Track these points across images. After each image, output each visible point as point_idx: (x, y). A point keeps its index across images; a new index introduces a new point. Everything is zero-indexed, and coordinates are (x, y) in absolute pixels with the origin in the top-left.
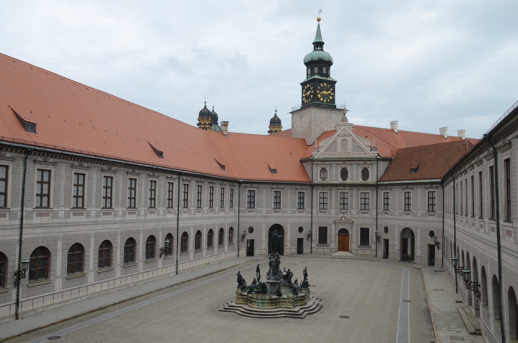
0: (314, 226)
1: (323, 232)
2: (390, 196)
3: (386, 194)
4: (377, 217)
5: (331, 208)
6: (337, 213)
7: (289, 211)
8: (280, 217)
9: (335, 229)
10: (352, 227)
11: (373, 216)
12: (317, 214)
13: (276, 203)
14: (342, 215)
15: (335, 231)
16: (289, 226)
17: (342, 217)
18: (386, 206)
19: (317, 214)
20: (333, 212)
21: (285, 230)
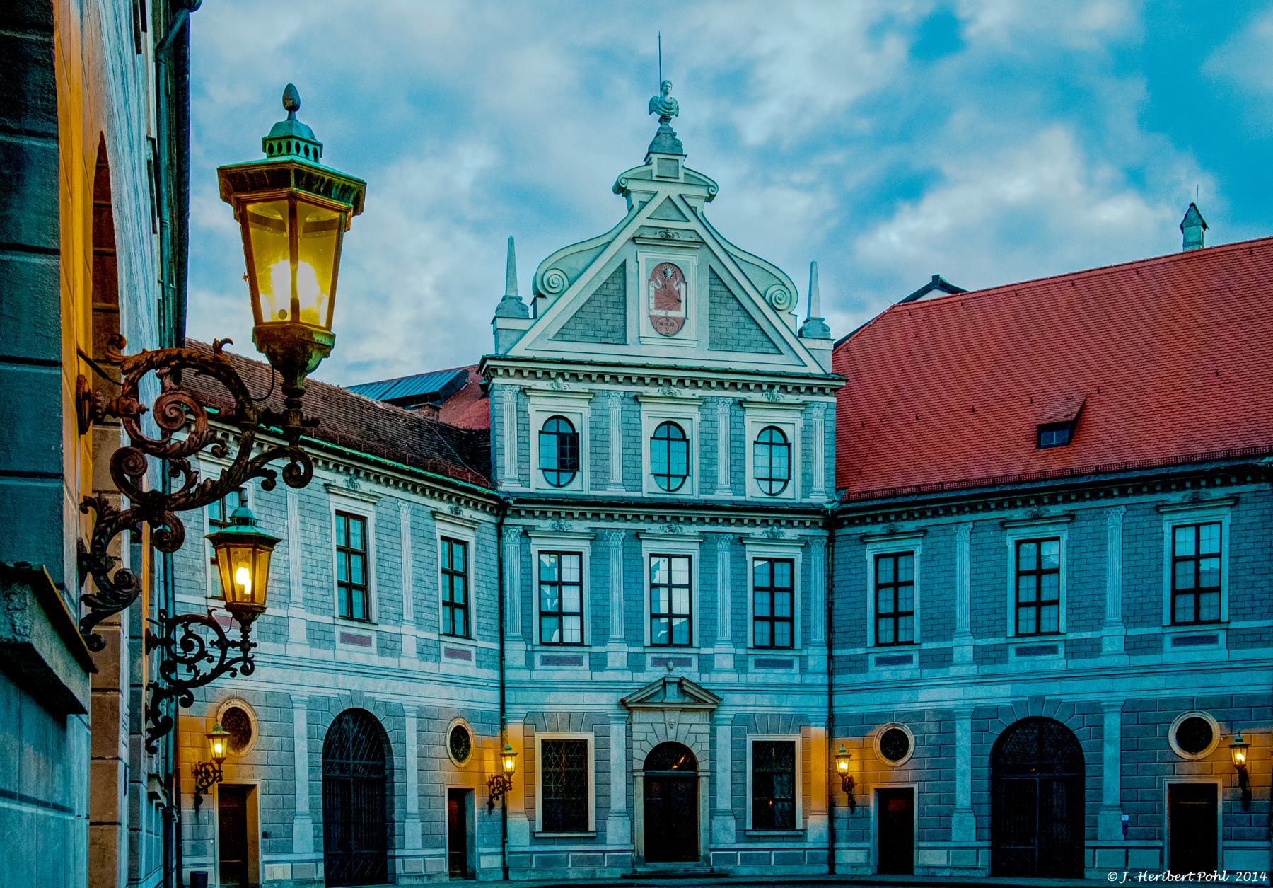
1: (566, 766)
2: (915, 569)
3: (887, 565)
4: (830, 685)
5: (602, 636)
6: (635, 664)
7: (409, 646)
9: (629, 748)
10: (713, 735)
11: (809, 679)
12: (529, 665)
14: (660, 672)
15: (629, 759)
17: (665, 684)
18: (887, 624)
20: (617, 653)
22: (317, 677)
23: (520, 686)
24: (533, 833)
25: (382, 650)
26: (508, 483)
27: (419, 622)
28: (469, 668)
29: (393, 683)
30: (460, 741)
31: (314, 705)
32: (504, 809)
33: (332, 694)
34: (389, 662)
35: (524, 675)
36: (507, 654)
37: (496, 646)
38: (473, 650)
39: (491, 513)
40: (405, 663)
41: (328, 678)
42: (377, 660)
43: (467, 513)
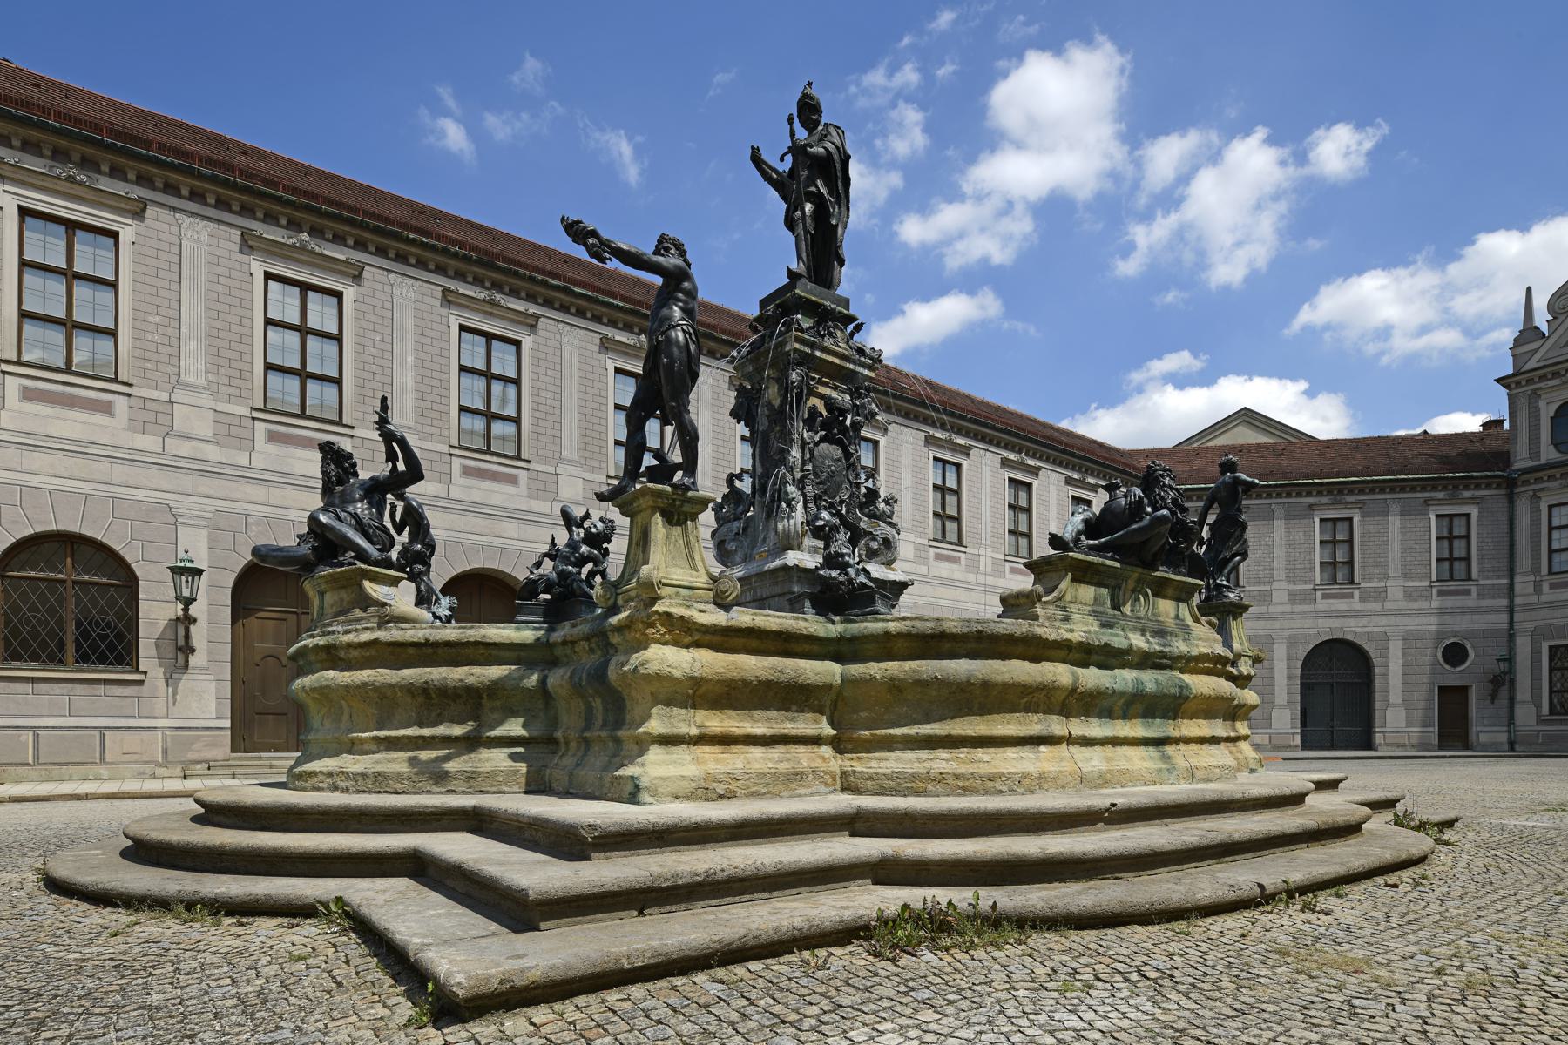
0: (1523, 645)
8: (1356, 615)
13: (1330, 565)
16: (1396, 648)
19: (1538, 589)
21: (1377, 661)
22: (1298, 623)
23: (1527, 608)
24: (1539, 716)
25: (1363, 600)
26: (1521, 460)
27: (1407, 575)
28: (1471, 601)
29: (1376, 620)
30: (1455, 654)
31: (1292, 641)
32: (1512, 700)
33: (1311, 631)
34: (1377, 606)
35: (1534, 599)
36: (1517, 588)
37: (1505, 581)
38: (1474, 589)
39: (1499, 487)
40: (1388, 605)
41: (1309, 622)
42: (1358, 607)
43: (1467, 494)
